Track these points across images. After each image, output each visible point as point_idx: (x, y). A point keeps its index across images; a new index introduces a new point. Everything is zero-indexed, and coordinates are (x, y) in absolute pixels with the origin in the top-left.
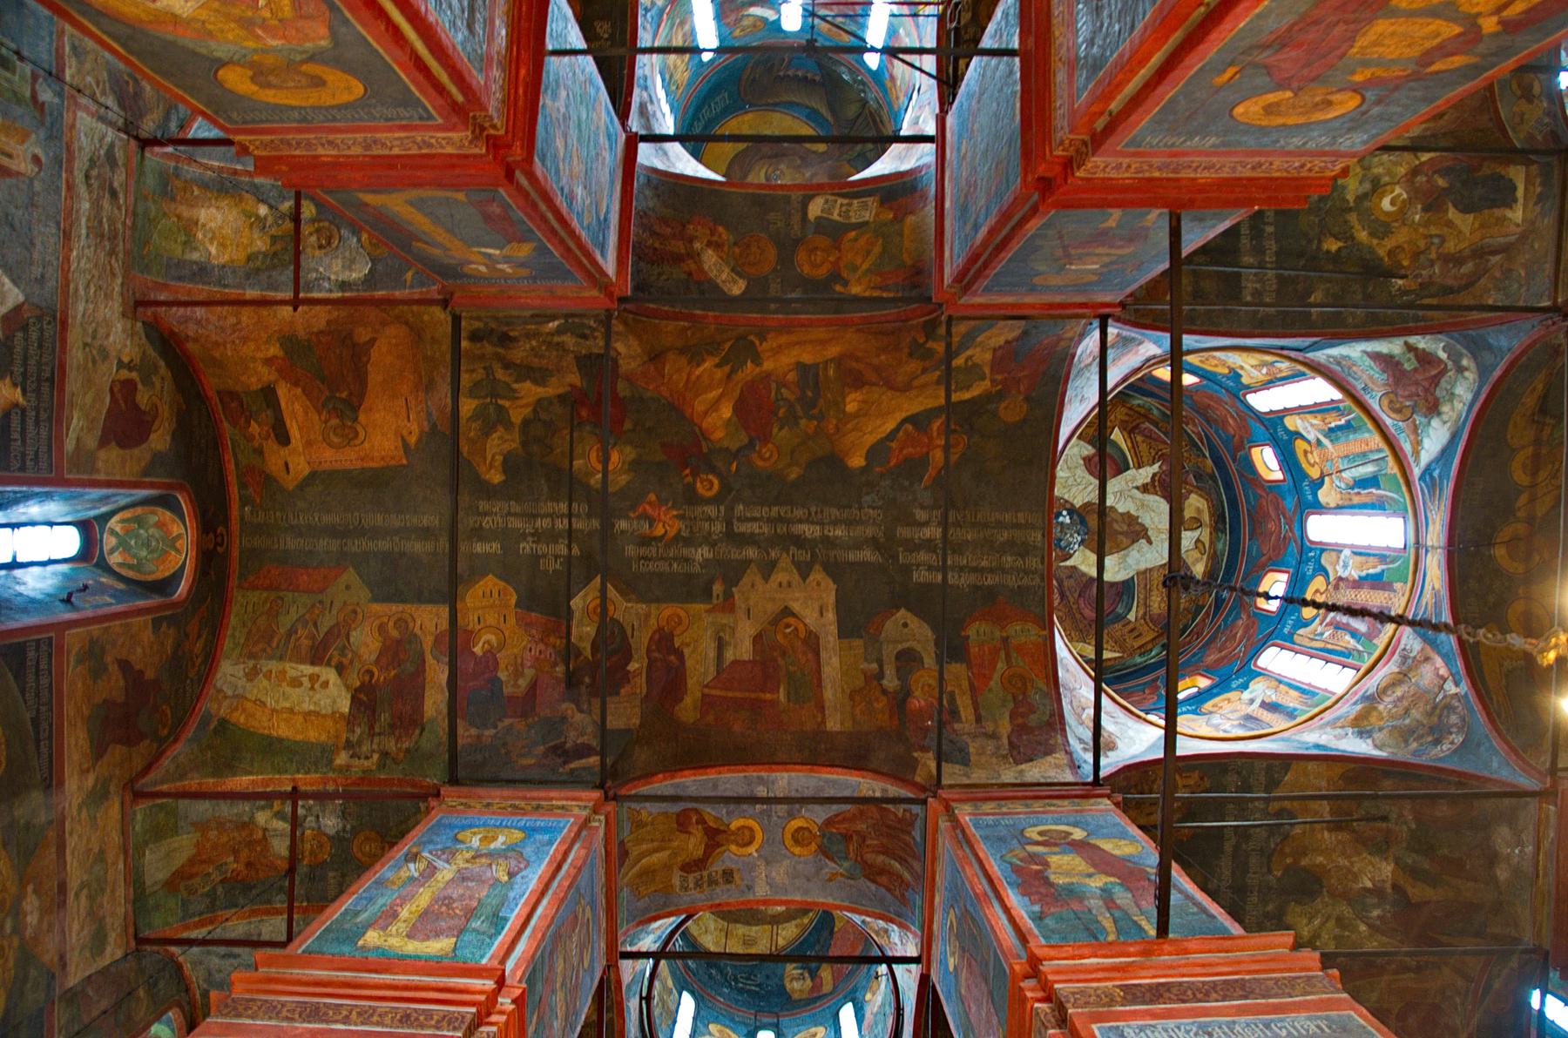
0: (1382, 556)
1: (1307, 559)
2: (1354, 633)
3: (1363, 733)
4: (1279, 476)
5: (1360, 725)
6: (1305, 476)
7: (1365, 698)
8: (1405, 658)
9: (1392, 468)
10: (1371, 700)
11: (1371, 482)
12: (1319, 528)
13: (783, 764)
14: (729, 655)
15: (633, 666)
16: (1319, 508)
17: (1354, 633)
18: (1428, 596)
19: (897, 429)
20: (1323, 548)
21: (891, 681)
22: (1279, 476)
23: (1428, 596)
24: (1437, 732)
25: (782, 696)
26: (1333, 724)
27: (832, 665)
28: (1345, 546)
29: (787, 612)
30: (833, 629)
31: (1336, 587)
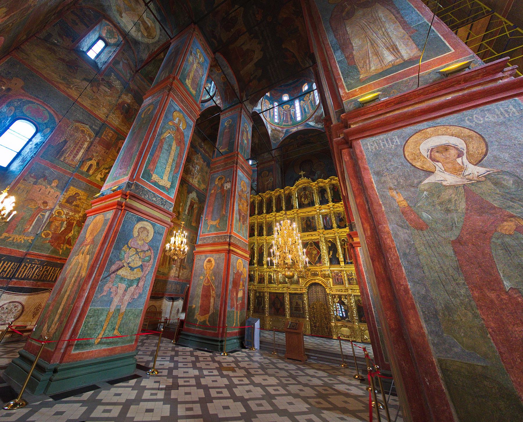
0: (295, 117)
1: (291, 101)
2: (283, 118)
3: (271, 131)
4: (303, 91)
5: (272, 130)
6: (304, 97)
7: (276, 129)
8: (282, 131)
9: (308, 115)
10: (276, 130)
11: (305, 112)
12: (297, 103)
13: (232, 69)
14: (243, 47)
15: (232, 30)
16: (300, 102)
17: (283, 118)
18: (291, 130)
19: (291, 52)
20: (294, 105)
21: (252, 78)
22: (303, 91)
23: (291, 130)
24: (275, 140)
25: (241, 61)
26: (271, 127)
27: (250, 66)
28: (295, 109)
29: (254, 51)
30: (255, 62)
31: (289, 110)
